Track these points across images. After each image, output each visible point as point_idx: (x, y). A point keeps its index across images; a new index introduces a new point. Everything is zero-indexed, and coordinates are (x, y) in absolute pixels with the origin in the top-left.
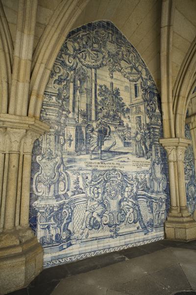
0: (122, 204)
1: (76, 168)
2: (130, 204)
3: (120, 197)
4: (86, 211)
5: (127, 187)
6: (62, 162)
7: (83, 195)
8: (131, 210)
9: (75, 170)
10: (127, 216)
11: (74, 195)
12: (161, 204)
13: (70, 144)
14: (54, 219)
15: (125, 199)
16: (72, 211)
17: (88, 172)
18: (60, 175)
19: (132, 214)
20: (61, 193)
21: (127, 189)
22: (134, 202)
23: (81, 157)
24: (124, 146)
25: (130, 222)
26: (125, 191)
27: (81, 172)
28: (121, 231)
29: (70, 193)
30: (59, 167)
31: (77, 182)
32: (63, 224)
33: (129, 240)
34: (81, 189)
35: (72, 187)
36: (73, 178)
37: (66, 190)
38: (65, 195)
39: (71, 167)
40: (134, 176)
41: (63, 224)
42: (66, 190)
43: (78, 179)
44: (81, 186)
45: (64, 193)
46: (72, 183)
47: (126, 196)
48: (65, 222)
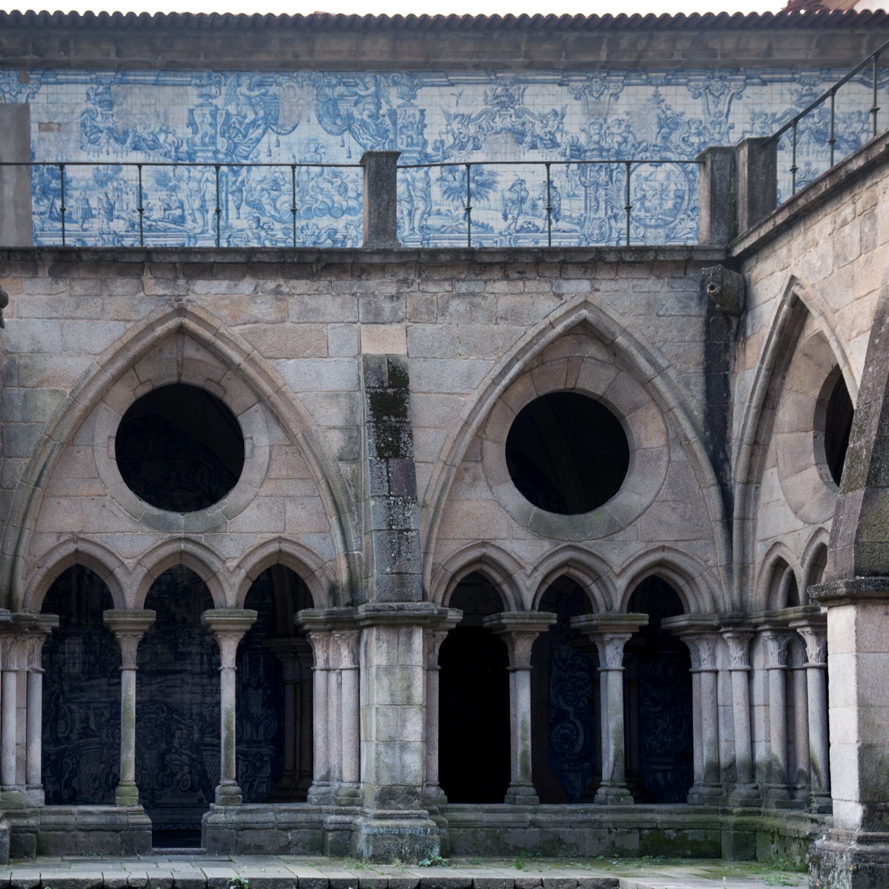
0: (168, 757)
1: (84, 700)
2: (185, 759)
3: (163, 746)
4: (101, 763)
5: (180, 729)
6: (63, 692)
7: (97, 739)
8: (186, 769)
9: (81, 702)
10: (178, 777)
11: (81, 738)
12: (258, 764)
13: (74, 664)
14: (51, 770)
15: (173, 750)
16: (78, 763)
17: (103, 705)
18: (58, 711)
19: (188, 776)
20: (60, 735)
21: (178, 733)
22: (194, 756)
23: (93, 682)
24: (176, 659)
25: (184, 789)
26: (173, 736)
27: (93, 705)
28: (163, 801)
29: (74, 737)
30: (58, 698)
31: (85, 720)
32: (64, 779)
33: (179, 817)
34: (93, 731)
35: (78, 726)
36: (78, 713)
37: (68, 732)
38: (68, 738)
39: (75, 698)
40: (195, 712)
41: (64, 779)
42: (68, 732)
43: (87, 715)
44: (93, 727)
45: (64, 735)
46: (77, 721)
47: (176, 746)
48: (67, 776)
